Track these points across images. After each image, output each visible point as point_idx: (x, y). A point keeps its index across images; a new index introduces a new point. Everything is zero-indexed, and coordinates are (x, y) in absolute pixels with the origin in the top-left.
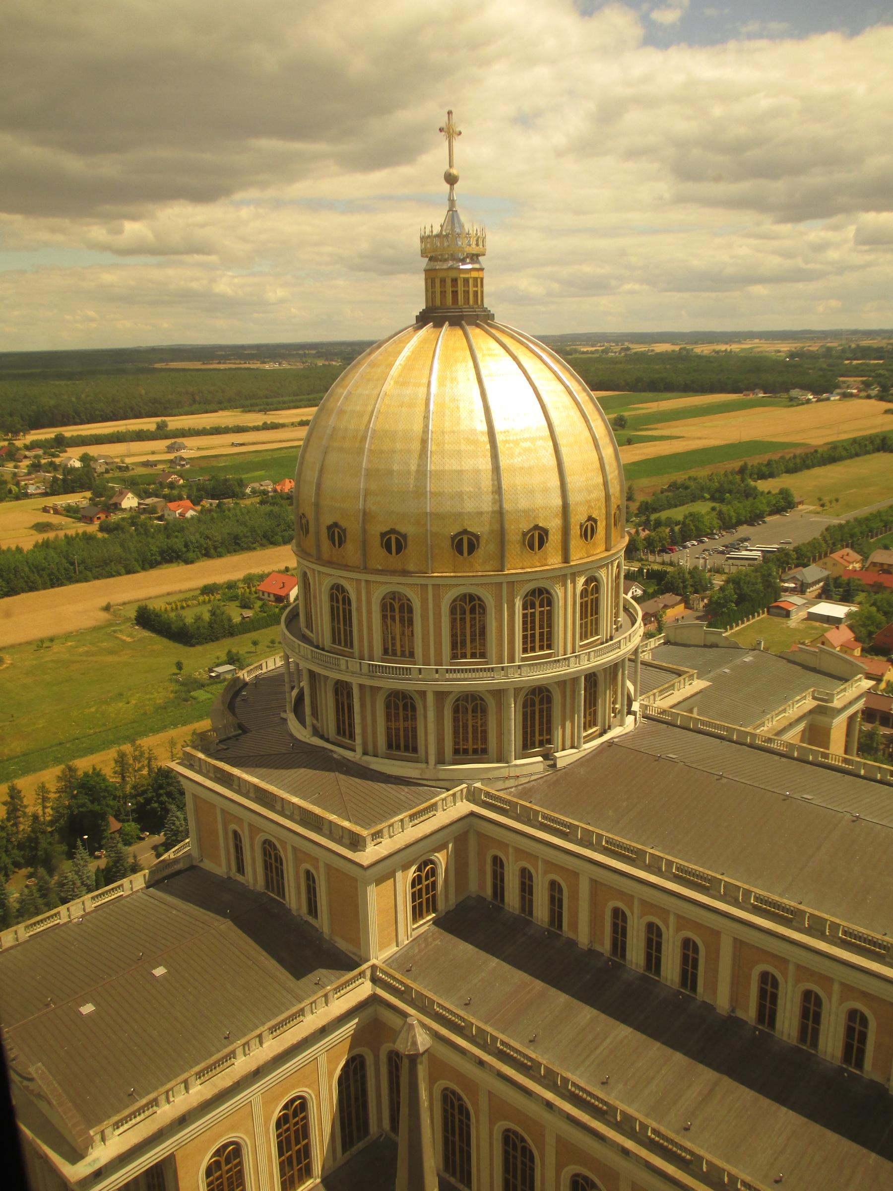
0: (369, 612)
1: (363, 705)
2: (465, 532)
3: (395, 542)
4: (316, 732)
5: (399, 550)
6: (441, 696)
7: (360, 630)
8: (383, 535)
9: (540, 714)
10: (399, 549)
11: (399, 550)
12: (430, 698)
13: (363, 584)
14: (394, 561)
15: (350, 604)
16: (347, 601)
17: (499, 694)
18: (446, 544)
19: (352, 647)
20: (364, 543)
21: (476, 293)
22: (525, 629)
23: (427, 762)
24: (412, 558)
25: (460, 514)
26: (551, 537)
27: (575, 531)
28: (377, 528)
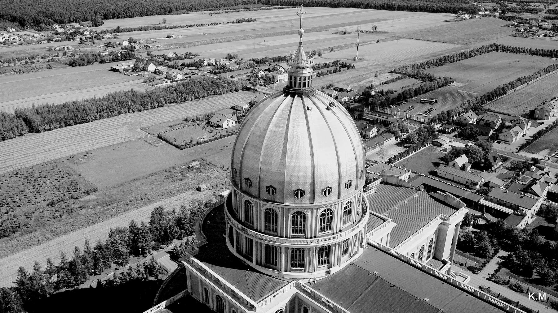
0: (260, 214)
3: (271, 190)
5: (273, 194)
9: (325, 253)
11: (273, 194)
14: (270, 197)
16: (251, 207)
17: (310, 249)
19: (253, 224)
20: (259, 189)
21: (309, 82)
22: (321, 223)
24: (277, 197)
25: (298, 183)
27: (343, 186)
28: (264, 185)
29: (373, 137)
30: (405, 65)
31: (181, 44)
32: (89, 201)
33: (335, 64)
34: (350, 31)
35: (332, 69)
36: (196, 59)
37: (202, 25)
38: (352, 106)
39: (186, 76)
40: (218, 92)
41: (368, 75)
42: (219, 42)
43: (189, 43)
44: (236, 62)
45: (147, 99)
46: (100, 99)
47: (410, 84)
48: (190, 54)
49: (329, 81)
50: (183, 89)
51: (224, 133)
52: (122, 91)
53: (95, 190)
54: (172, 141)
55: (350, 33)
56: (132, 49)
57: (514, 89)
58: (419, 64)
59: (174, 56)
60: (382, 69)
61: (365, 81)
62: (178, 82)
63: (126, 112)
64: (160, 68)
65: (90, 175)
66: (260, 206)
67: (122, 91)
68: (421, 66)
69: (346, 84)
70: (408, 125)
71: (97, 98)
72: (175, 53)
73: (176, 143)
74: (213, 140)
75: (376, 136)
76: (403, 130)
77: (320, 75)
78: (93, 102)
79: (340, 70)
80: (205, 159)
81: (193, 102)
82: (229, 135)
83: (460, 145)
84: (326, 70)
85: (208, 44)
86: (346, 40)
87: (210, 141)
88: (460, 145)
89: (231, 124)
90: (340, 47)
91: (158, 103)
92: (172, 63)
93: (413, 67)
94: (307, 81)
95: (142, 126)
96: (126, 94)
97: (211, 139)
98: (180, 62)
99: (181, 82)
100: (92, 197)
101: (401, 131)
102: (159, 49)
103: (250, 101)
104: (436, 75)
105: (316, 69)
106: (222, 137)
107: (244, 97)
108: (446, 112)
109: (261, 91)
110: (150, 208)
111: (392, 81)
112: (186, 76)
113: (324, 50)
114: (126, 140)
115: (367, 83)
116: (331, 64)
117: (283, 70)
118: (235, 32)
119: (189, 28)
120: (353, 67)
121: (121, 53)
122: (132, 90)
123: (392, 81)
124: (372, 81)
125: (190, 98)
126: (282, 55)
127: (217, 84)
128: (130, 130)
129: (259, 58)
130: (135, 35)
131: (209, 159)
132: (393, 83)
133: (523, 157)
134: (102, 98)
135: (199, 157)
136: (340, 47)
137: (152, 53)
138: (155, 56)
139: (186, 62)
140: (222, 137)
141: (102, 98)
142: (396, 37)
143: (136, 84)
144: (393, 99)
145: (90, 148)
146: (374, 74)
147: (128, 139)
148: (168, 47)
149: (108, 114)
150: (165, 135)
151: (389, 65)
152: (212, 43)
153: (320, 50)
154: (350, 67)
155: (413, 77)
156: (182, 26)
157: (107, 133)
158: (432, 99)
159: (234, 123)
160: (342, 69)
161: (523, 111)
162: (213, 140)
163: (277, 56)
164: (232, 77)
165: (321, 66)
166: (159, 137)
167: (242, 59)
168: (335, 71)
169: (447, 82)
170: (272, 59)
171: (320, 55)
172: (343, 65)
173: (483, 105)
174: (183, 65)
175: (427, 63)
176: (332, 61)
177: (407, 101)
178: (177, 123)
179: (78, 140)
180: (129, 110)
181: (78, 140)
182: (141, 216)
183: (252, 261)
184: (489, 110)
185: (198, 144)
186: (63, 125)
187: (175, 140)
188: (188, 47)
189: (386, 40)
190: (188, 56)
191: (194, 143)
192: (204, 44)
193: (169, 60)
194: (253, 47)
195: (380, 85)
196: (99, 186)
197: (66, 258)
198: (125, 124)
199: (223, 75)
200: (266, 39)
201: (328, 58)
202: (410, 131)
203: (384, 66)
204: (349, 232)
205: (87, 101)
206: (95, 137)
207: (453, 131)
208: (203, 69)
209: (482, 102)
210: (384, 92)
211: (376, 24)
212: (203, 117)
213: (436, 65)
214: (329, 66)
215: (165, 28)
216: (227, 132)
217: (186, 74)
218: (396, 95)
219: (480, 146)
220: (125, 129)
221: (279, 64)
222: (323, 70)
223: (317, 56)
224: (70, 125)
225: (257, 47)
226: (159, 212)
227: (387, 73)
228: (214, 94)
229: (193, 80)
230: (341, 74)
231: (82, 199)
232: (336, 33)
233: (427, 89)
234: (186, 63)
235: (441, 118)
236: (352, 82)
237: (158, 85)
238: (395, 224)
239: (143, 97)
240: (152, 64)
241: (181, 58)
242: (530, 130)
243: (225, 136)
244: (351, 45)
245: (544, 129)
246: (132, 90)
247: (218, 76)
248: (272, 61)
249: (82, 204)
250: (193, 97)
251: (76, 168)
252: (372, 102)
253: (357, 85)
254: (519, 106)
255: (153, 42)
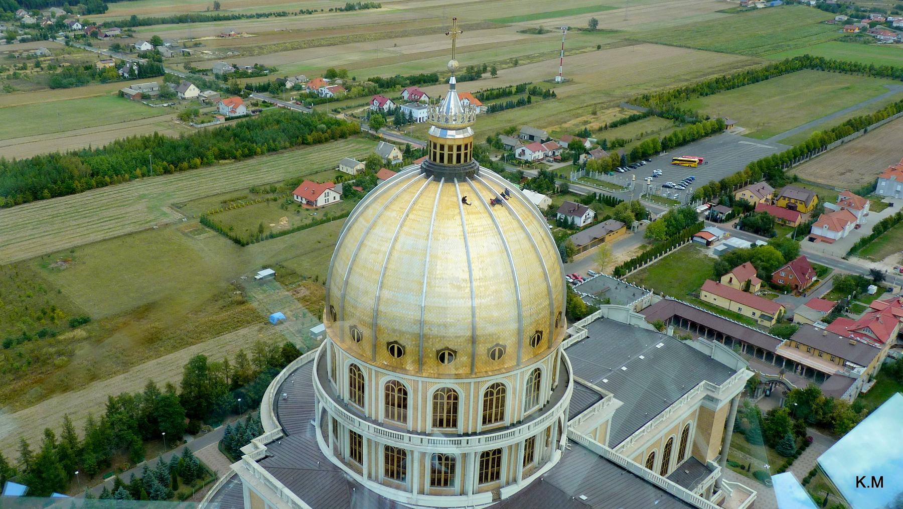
1: (369, 453)
2: (447, 349)
4: (337, 453)
6: (423, 454)
7: (370, 398)
8: (389, 344)
10: (400, 354)
12: (416, 455)
13: (373, 372)
15: (363, 379)
18: (432, 355)
23: (412, 492)
26: (507, 350)
29: (585, 227)
30: (646, 92)
31: (245, 49)
32: (73, 341)
33: (520, 89)
34: (548, 28)
35: (515, 99)
36: (272, 78)
37: (284, 14)
38: (551, 169)
39: (254, 108)
40: (310, 138)
41: (580, 111)
42: (314, 46)
43: (260, 48)
44: (344, 84)
45: (181, 152)
46: (97, 151)
47: (656, 129)
48: (262, 68)
49: (509, 121)
50: (248, 134)
51: (318, 216)
52: (138, 136)
53: (85, 321)
54: (226, 230)
55: (548, 32)
56: (156, 57)
57: (839, 141)
58: (671, 91)
59: (233, 70)
60: (605, 99)
61: (573, 122)
62: (239, 120)
63: (143, 175)
64: (207, 93)
65: (79, 293)
66: (377, 376)
67: (138, 136)
68: (677, 94)
69: (540, 128)
70: (648, 205)
71: (93, 148)
72: (235, 66)
73: (232, 234)
74: (299, 229)
75: (591, 225)
76: (641, 215)
77: (493, 110)
78: (83, 155)
79: (529, 102)
80: (284, 264)
81: (265, 158)
82: (328, 220)
83: (741, 243)
84: (504, 101)
85: (293, 49)
86: (544, 44)
87: (293, 231)
88: (741, 243)
89: (331, 200)
90: (530, 58)
91: (202, 159)
92: (229, 85)
93: (660, 97)
94: (463, 152)
95: (172, 201)
96: (146, 142)
97: (295, 227)
98: (242, 83)
99: (244, 120)
100: (80, 333)
101: (636, 215)
102: (206, 57)
103: (366, 156)
104: (702, 112)
105: (488, 99)
106: (316, 223)
107: (357, 150)
108: (717, 182)
109: (388, 138)
110: (184, 357)
111: (623, 122)
112: (254, 108)
113: (502, 63)
114: (142, 228)
115: (577, 125)
116: (514, 90)
117: (427, 99)
118: (342, 28)
119: (261, 19)
120: (554, 95)
121: (138, 64)
122: (156, 134)
123: (623, 122)
124: (586, 123)
125: (259, 150)
126: (427, 72)
127: (307, 125)
128: (151, 209)
129: (386, 76)
130: (159, 31)
131: (291, 265)
132: (623, 127)
133: (852, 268)
134: (101, 148)
135: (272, 261)
136: (530, 58)
137: (193, 65)
138: (199, 71)
139: (255, 82)
140: (316, 223)
141: (101, 148)
142: (632, 41)
143: (167, 125)
144: (623, 156)
145: (78, 242)
146: (590, 109)
147: (147, 226)
148: (222, 55)
149: (111, 177)
150: (215, 219)
151: (618, 93)
152: (301, 48)
153: (495, 63)
154: (548, 95)
155: (661, 115)
156: (248, 14)
157: (111, 213)
158: (694, 155)
159: (338, 198)
160: (533, 98)
161: (857, 181)
162: (299, 229)
163: (417, 73)
164: (336, 111)
165: (495, 92)
166: (205, 222)
167: (354, 79)
168: (521, 103)
169: (719, 128)
170: (408, 78)
171: (494, 72)
172: (534, 92)
173: (785, 170)
174: (249, 88)
175: (687, 90)
176: (515, 85)
177: (647, 160)
178: (235, 195)
179: (56, 226)
180: (149, 171)
181: (56, 226)
182: (167, 372)
183: (361, 474)
184: (796, 179)
185: (272, 236)
186: (31, 198)
187: (231, 229)
188: (259, 54)
189: (613, 46)
190: (259, 71)
191: (264, 235)
192: (286, 49)
193: (225, 78)
194: (374, 56)
195: (601, 129)
196: (94, 312)
197: (30, 449)
198: (141, 197)
199: (320, 109)
200: (397, 41)
201: (508, 78)
202: (653, 216)
203: (607, 94)
204: (536, 425)
205: (75, 154)
206: (87, 220)
207: (730, 217)
208: (284, 96)
209: (783, 164)
210: (609, 145)
211: (596, 16)
212: (282, 185)
213: (701, 94)
214: (510, 94)
215: (216, 19)
216: (326, 215)
217: (256, 105)
218: (627, 150)
219: (778, 246)
220: (141, 206)
221: (422, 89)
222: (498, 102)
223: (488, 75)
224: (43, 198)
225: (381, 55)
226: (199, 366)
227: (614, 107)
228: (303, 143)
229: (266, 117)
230: (532, 108)
231: (61, 338)
232: (523, 32)
233: (684, 139)
234: (254, 85)
235: (708, 194)
236: (550, 124)
237: (202, 125)
238: (617, 403)
239: (174, 146)
240: (192, 87)
241: (244, 75)
242: (868, 218)
243: (322, 222)
244: (551, 55)
245: (893, 215)
246: (156, 134)
247: (311, 111)
248: (408, 82)
249: (61, 347)
250: (265, 148)
251: (51, 278)
252: (585, 164)
253: (558, 130)
254: (850, 171)
255: (196, 45)
